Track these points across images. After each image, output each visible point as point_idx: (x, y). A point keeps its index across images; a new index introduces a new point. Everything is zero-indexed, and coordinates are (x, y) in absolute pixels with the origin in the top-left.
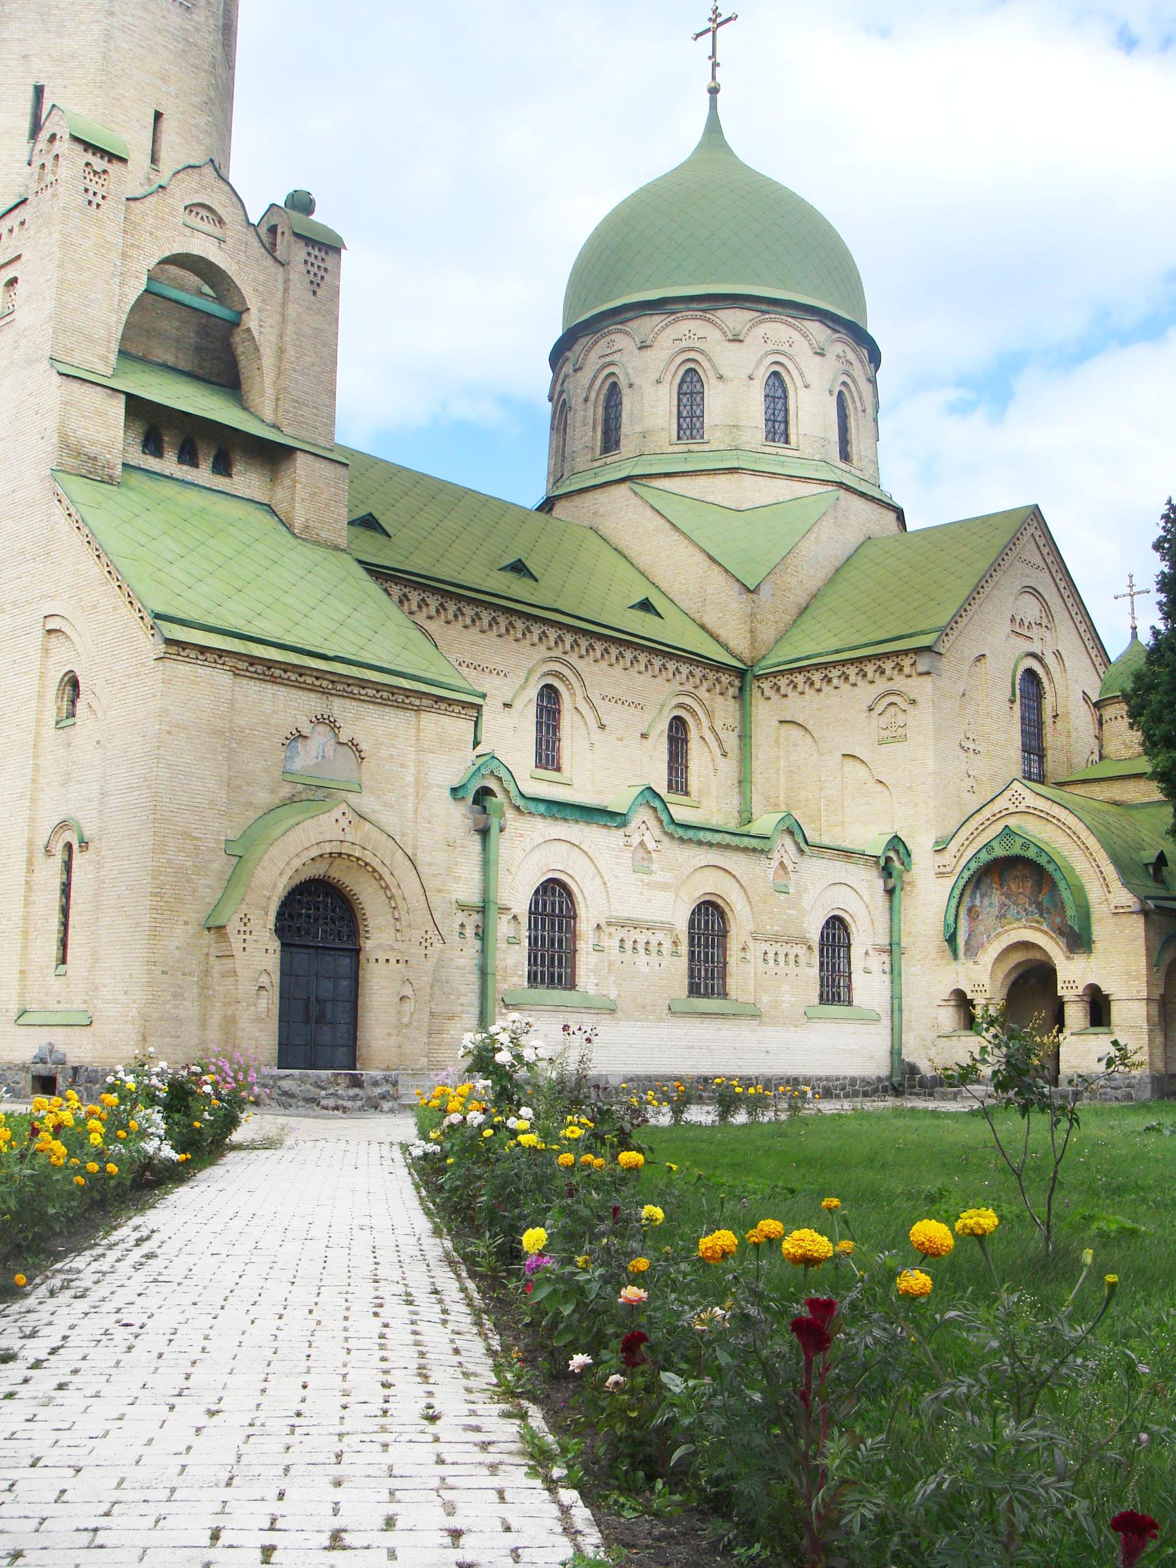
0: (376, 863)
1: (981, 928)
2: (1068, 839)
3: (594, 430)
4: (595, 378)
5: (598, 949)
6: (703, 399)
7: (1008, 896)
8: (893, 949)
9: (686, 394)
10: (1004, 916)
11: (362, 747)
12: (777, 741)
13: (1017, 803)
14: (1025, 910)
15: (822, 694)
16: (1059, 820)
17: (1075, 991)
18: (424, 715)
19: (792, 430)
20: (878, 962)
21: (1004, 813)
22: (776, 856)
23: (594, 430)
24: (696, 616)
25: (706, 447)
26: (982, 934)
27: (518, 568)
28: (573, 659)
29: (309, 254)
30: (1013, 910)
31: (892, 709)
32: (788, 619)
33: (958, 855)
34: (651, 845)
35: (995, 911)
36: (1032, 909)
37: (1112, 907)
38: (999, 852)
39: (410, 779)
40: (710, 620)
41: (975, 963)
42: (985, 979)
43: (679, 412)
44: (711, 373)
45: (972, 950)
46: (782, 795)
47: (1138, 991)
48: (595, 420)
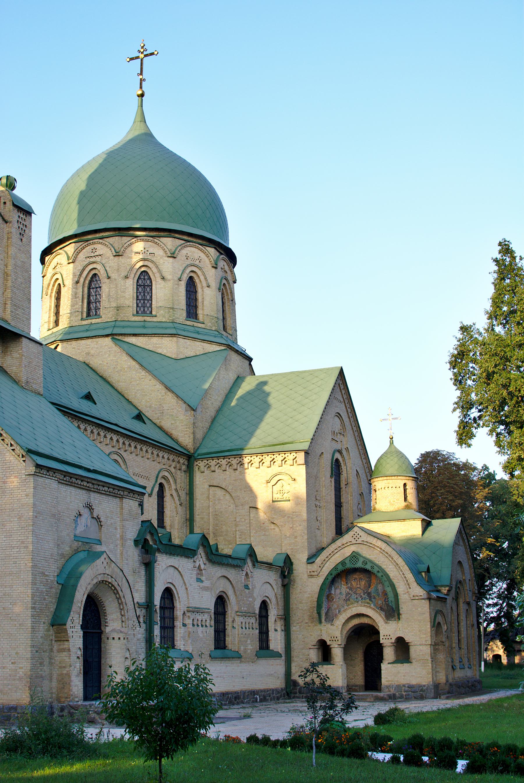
0: (115, 584)
2: (386, 559)
3: (83, 302)
4: (83, 270)
5: (184, 625)
6: (151, 289)
7: (351, 589)
8: (286, 618)
9: (140, 286)
10: (349, 600)
11: (102, 519)
12: (208, 497)
13: (357, 539)
15: (237, 472)
16: (381, 549)
17: (390, 641)
18: (124, 500)
19: (200, 312)
20: (280, 625)
22: (245, 569)
23: (83, 302)
24: (157, 421)
25: (155, 319)
26: (335, 609)
27: (88, 397)
28: (122, 452)
29: (19, 216)
30: (354, 596)
32: (207, 425)
33: (322, 566)
34: (202, 566)
35: (344, 597)
36: (365, 596)
37: (411, 596)
38: (349, 565)
39: (118, 536)
40: (166, 424)
42: (338, 634)
43: (137, 297)
44: (158, 275)
45: (330, 618)
46: (211, 528)
47: (426, 641)
48: (83, 295)
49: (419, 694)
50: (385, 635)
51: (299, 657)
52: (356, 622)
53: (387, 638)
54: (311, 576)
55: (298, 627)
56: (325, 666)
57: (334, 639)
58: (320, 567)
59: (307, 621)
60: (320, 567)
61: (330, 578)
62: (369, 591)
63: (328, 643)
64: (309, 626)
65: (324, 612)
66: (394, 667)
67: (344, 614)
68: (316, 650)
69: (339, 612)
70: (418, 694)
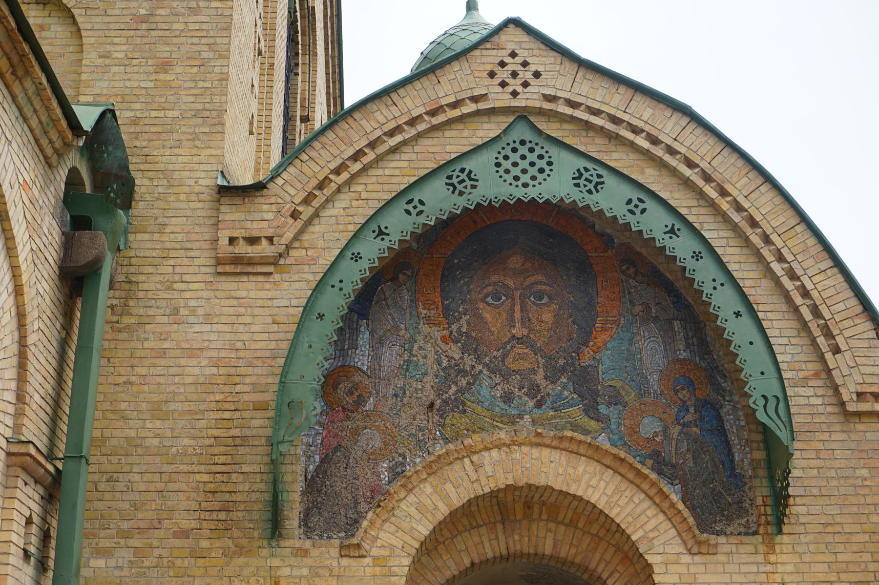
1: (372, 439)
7: (471, 345)
10: (458, 405)
13: (515, 84)
14: (534, 391)
16: (655, 141)
21: (470, 107)
26: (373, 458)
30: (488, 389)
33: (306, 212)
38: (493, 186)
41: (345, 550)
52: (482, 545)
54: (237, 260)
55: (124, 556)
58: (295, 215)
59: (185, 524)
60: (295, 215)
61: (353, 275)
62: (586, 361)
64: (197, 554)
65: (299, 468)
67: (428, 488)
69: (396, 473)
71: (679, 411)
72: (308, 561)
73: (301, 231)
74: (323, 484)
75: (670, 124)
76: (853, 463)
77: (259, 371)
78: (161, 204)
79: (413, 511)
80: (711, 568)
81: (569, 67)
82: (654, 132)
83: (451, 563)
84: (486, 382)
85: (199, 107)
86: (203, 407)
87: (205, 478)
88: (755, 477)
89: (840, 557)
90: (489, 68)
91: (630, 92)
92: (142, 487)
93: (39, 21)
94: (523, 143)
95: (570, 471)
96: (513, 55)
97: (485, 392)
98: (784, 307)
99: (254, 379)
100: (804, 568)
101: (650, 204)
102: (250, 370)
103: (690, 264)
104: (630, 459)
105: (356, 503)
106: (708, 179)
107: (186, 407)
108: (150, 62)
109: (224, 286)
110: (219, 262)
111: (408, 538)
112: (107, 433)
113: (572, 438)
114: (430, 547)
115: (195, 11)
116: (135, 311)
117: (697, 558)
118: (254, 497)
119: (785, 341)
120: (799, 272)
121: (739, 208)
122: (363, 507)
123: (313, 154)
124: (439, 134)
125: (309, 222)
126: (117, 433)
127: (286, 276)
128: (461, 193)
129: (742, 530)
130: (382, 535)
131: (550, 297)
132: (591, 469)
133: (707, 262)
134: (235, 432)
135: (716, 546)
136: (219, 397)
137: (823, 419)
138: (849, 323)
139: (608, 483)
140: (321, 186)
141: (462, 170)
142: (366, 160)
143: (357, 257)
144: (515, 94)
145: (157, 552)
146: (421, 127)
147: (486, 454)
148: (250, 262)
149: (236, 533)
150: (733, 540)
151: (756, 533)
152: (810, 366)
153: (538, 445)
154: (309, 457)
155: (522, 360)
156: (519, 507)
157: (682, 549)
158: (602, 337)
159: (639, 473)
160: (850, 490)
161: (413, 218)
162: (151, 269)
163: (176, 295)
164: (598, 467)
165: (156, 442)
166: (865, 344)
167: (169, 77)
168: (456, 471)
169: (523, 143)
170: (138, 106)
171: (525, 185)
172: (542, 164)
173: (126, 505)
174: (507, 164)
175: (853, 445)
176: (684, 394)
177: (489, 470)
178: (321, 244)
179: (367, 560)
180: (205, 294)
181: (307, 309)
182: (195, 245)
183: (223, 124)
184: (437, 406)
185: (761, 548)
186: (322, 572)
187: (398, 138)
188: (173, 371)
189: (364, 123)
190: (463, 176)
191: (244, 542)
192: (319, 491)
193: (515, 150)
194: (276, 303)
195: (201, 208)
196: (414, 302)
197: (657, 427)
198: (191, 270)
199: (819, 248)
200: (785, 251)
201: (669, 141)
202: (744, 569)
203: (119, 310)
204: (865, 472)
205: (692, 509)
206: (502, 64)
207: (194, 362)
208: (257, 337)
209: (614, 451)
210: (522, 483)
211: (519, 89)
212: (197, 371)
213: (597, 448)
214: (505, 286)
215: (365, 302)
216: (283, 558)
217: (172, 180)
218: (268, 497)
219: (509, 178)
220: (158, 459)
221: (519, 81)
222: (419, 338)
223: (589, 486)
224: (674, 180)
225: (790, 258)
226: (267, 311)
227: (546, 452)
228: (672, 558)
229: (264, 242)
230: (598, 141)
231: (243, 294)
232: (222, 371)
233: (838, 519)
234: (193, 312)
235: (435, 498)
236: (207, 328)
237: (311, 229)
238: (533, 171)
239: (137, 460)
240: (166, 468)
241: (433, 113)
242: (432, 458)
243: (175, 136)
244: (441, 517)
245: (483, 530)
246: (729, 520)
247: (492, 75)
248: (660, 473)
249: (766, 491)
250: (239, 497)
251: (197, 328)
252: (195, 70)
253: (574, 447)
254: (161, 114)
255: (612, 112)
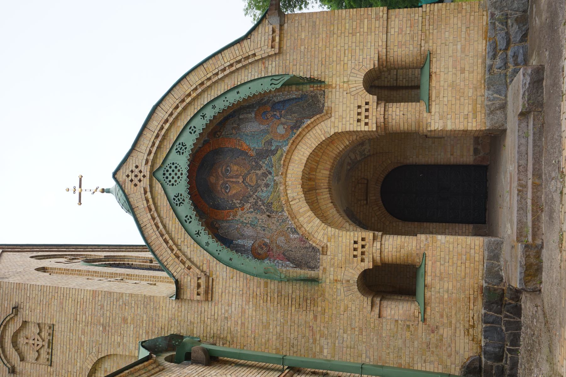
1: (281, 240)
7: (245, 199)
10: (269, 205)
13: (140, 176)
14: (265, 175)
16: (167, 121)
17: (373, 105)
21: (149, 194)
26: (288, 240)
30: (263, 193)
31: (21, 340)
33: (188, 263)
36: (264, 163)
38: (181, 187)
41: (324, 253)
47: (377, 18)
49: (516, 27)
50: (356, 117)
51: (400, 349)
52: (325, 198)
53: (364, 114)
54: (207, 292)
56: (429, 279)
57: (360, 250)
58: (189, 268)
59: (311, 316)
60: (189, 268)
61: (214, 245)
62: (254, 153)
63: (368, 265)
64: (324, 312)
65: (291, 270)
66: (438, 97)
67: (301, 219)
68: (385, 303)
69: (295, 231)
70: (514, 29)
71: (275, 118)
72: (328, 268)
73: (196, 266)
74: (298, 260)
75: (160, 114)
76: (299, 52)
77: (252, 285)
78: (182, 323)
79: (310, 225)
80: (337, 110)
81: (134, 154)
82: (163, 121)
83: (331, 211)
84: (260, 194)
85: (142, 306)
86: (265, 308)
87: (293, 308)
88: (302, 90)
89: (335, 59)
90: (133, 186)
91: (146, 129)
92: (296, 333)
93: (103, 372)
94: (164, 174)
95: (297, 162)
96: (128, 176)
97: (264, 194)
98: (236, 74)
99: (255, 287)
100: (338, 73)
101: (192, 125)
102: (251, 289)
103: (217, 110)
104: (293, 138)
105: (306, 248)
106: (183, 101)
107: (265, 315)
108: (123, 326)
109: (217, 298)
110: (207, 300)
111: (321, 228)
112: (274, 347)
113: (284, 161)
114: (324, 219)
115: (102, 307)
116: (225, 335)
117: (333, 115)
118: (302, 289)
119: (250, 75)
120: (223, 67)
121: (196, 89)
122: (307, 245)
123: (164, 260)
124: (159, 208)
125: (192, 262)
126: (274, 343)
127: (214, 273)
128: (184, 200)
129: (323, 96)
130: (319, 238)
131: (228, 167)
132: (296, 154)
133: (216, 103)
134: (276, 295)
135: (328, 107)
136: (262, 302)
137: (281, 62)
138: (244, 49)
139: (302, 148)
140: (178, 257)
141: (174, 199)
142: (168, 238)
143: (207, 244)
144: (144, 176)
145: (322, 328)
146: (156, 215)
147: (289, 195)
148: (207, 287)
149: (316, 296)
150: (326, 100)
151: (324, 91)
152: (260, 65)
153: (286, 174)
154: (287, 266)
155: (252, 179)
156: (310, 183)
157: (329, 120)
158: (245, 146)
159: (299, 135)
160: (309, 54)
161: (193, 220)
162: (209, 328)
163: (219, 318)
164: (296, 151)
165: (278, 328)
166: (252, 44)
167: (129, 318)
168: (295, 208)
169: (164, 174)
170: (141, 332)
171: (182, 174)
172: (173, 167)
173: (303, 340)
174: (173, 181)
175: (292, 51)
176: (269, 116)
177: (295, 194)
178: (201, 258)
179: (328, 244)
180: (220, 306)
181: (227, 265)
182: (200, 309)
183: (150, 296)
184: (269, 214)
185: (330, 90)
186: (332, 263)
187: (160, 225)
188: (250, 320)
189: (153, 238)
190: (177, 199)
191: (319, 293)
192: (301, 262)
193: (167, 178)
194: (225, 277)
195: (184, 307)
196: (227, 221)
197: (281, 127)
198: (210, 311)
199: (213, 58)
200: (214, 72)
201: (167, 115)
202: (337, 97)
203: (225, 341)
204: (302, 48)
205: (314, 115)
206: (132, 181)
207: (247, 311)
208: (238, 285)
209: (290, 144)
210: (301, 182)
211: (142, 174)
212: (251, 310)
213: (288, 151)
214: (222, 184)
215: (226, 241)
216: (326, 278)
217: (172, 318)
218: (302, 283)
219: (178, 180)
220: (285, 327)
221: (139, 174)
222: (241, 220)
223: (303, 155)
224: (183, 114)
225: (217, 71)
226: (228, 281)
227: (289, 171)
228: (332, 124)
229: (199, 281)
230: (165, 144)
231: (220, 290)
232: (251, 300)
233: (320, 59)
234: (227, 311)
235: (305, 216)
236: (233, 305)
237: (195, 262)
238: (176, 171)
239: (285, 336)
240: (289, 324)
241: (150, 210)
242: (289, 217)
243: (154, 316)
244: (313, 214)
245: (319, 198)
246: (319, 101)
247: (136, 185)
248: (299, 127)
249: (308, 86)
250: (302, 295)
251: (233, 309)
252: (127, 307)
253: (288, 160)
254: (145, 322)
255: (154, 137)
